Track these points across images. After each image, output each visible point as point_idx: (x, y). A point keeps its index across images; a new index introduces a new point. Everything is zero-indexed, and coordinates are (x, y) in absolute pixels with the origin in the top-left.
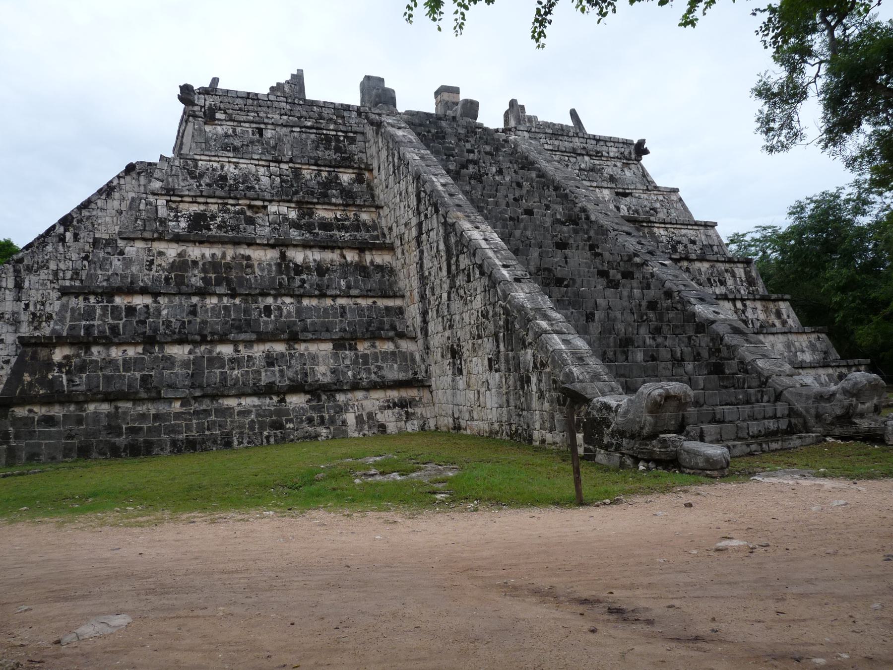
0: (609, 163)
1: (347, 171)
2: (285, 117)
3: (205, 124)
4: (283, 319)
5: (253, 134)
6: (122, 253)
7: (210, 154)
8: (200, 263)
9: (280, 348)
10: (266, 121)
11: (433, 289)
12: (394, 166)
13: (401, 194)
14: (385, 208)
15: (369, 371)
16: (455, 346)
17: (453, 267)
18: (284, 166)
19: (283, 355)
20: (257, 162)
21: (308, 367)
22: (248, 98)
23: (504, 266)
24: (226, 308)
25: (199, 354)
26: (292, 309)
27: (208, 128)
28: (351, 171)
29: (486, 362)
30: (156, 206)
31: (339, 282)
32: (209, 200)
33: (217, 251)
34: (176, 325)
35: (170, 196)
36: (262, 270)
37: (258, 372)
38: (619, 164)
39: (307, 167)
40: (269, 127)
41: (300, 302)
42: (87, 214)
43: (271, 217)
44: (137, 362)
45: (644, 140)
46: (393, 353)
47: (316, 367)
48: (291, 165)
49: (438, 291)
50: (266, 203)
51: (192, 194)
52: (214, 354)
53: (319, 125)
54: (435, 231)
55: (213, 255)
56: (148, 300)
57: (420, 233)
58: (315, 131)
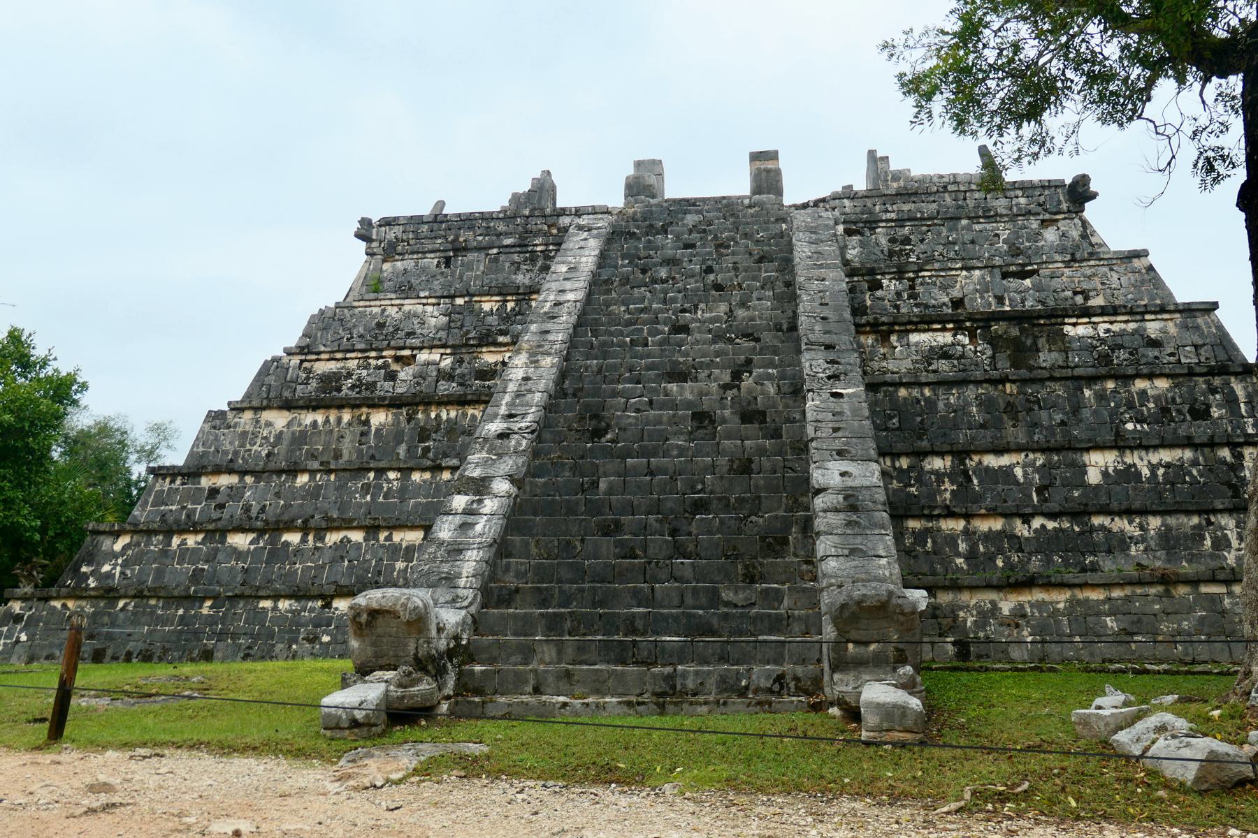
20: (424, 301)
27: (386, 266)
32: (348, 355)
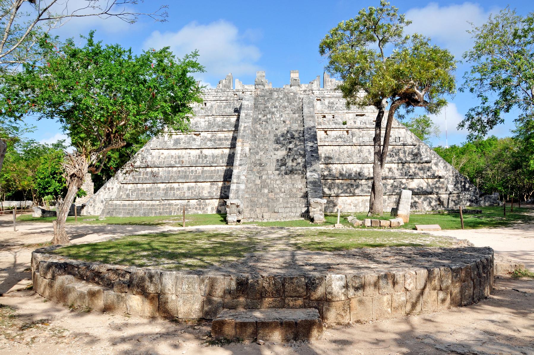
6: (151, 154)
9: (193, 184)
19: (193, 187)
24: (179, 171)
34: (163, 177)
37: (185, 192)
44: (150, 188)
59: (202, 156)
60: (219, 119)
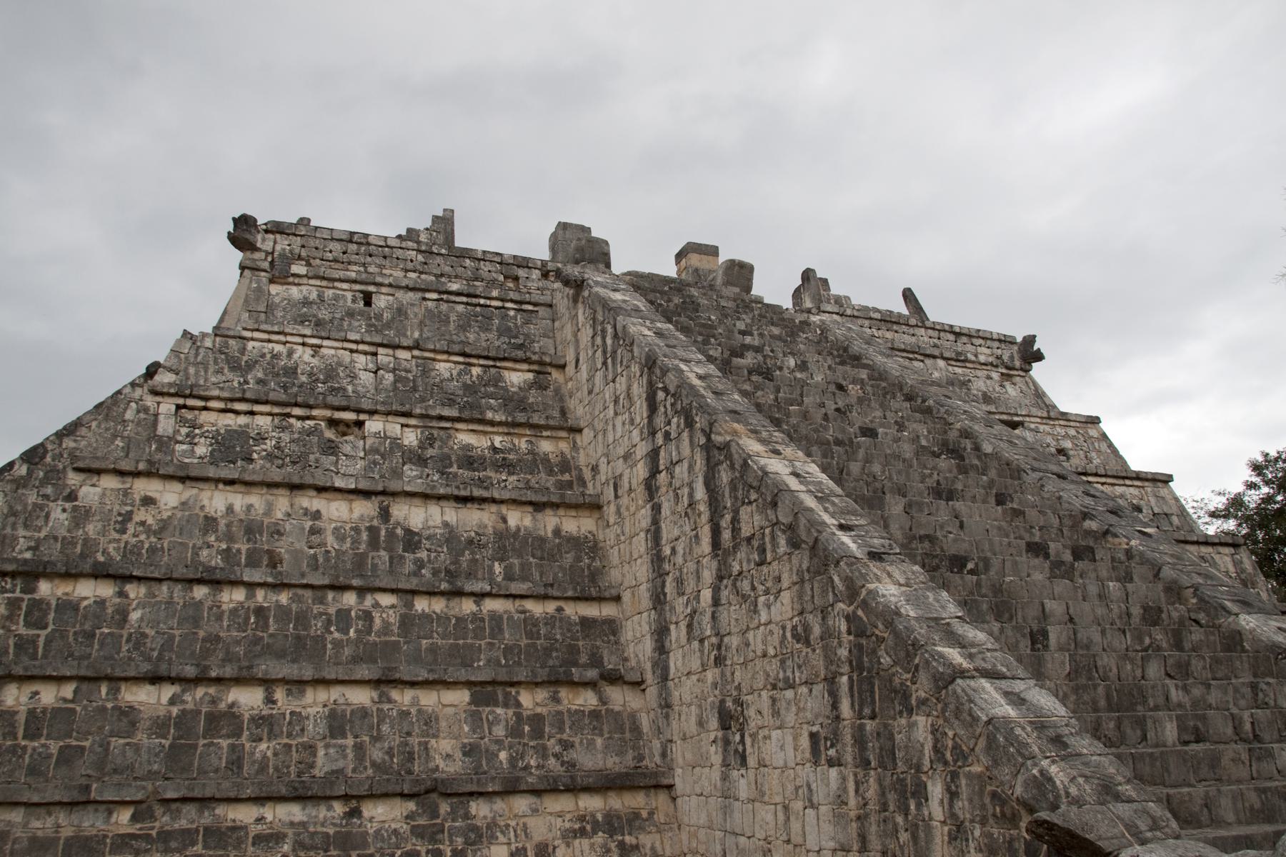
0: (979, 373)
1: (518, 366)
2: (413, 275)
3: (271, 281)
4: (373, 638)
5: (354, 301)
6: (72, 497)
7: (270, 329)
8: (222, 523)
9: (361, 697)
10: (379, 279)
11: (680, 582)
12: (604, 352)
13: (616, 402)
14: (586, 431)
15: (543, 752)
16: (729, 704)
17: (726, 535)
18: (403, 355)
19: (363, 712)
20: (354, 346)
21: (414, 741)
22: (351, 241)
23: (842, 527)
24: (260, 611)
25: (190, 706)
26: (393, 618)
27: (274, 289)
28: (525, 367)
29: (805, 742)
30: (156, 415)
31: (491, 568)
32: (257, 408)
33: (257, 500)
34: (154, 644)
35: (185, 397)
36: (341, 538)
37: (311, 748)
38: (995, 376)
39: (445, 357)
40: (384, 290)
41: (410, 605)
42: (72, 444)
43: (369, 442)
44: (62, 716)
45: (1034, 336)
46: (595, 714)
47: (433, 741)
48: (416, 353)
49: (690, 586)
50: (362, 417)
51: (226, 394)
52: (222, 706)
53: (472, 291)
54: (686, 464)
55: (250, 507)
56: (106, 590)
57: (654, 472)
58: (464, 299)
59: (391, 534)
60: (444, 368)
